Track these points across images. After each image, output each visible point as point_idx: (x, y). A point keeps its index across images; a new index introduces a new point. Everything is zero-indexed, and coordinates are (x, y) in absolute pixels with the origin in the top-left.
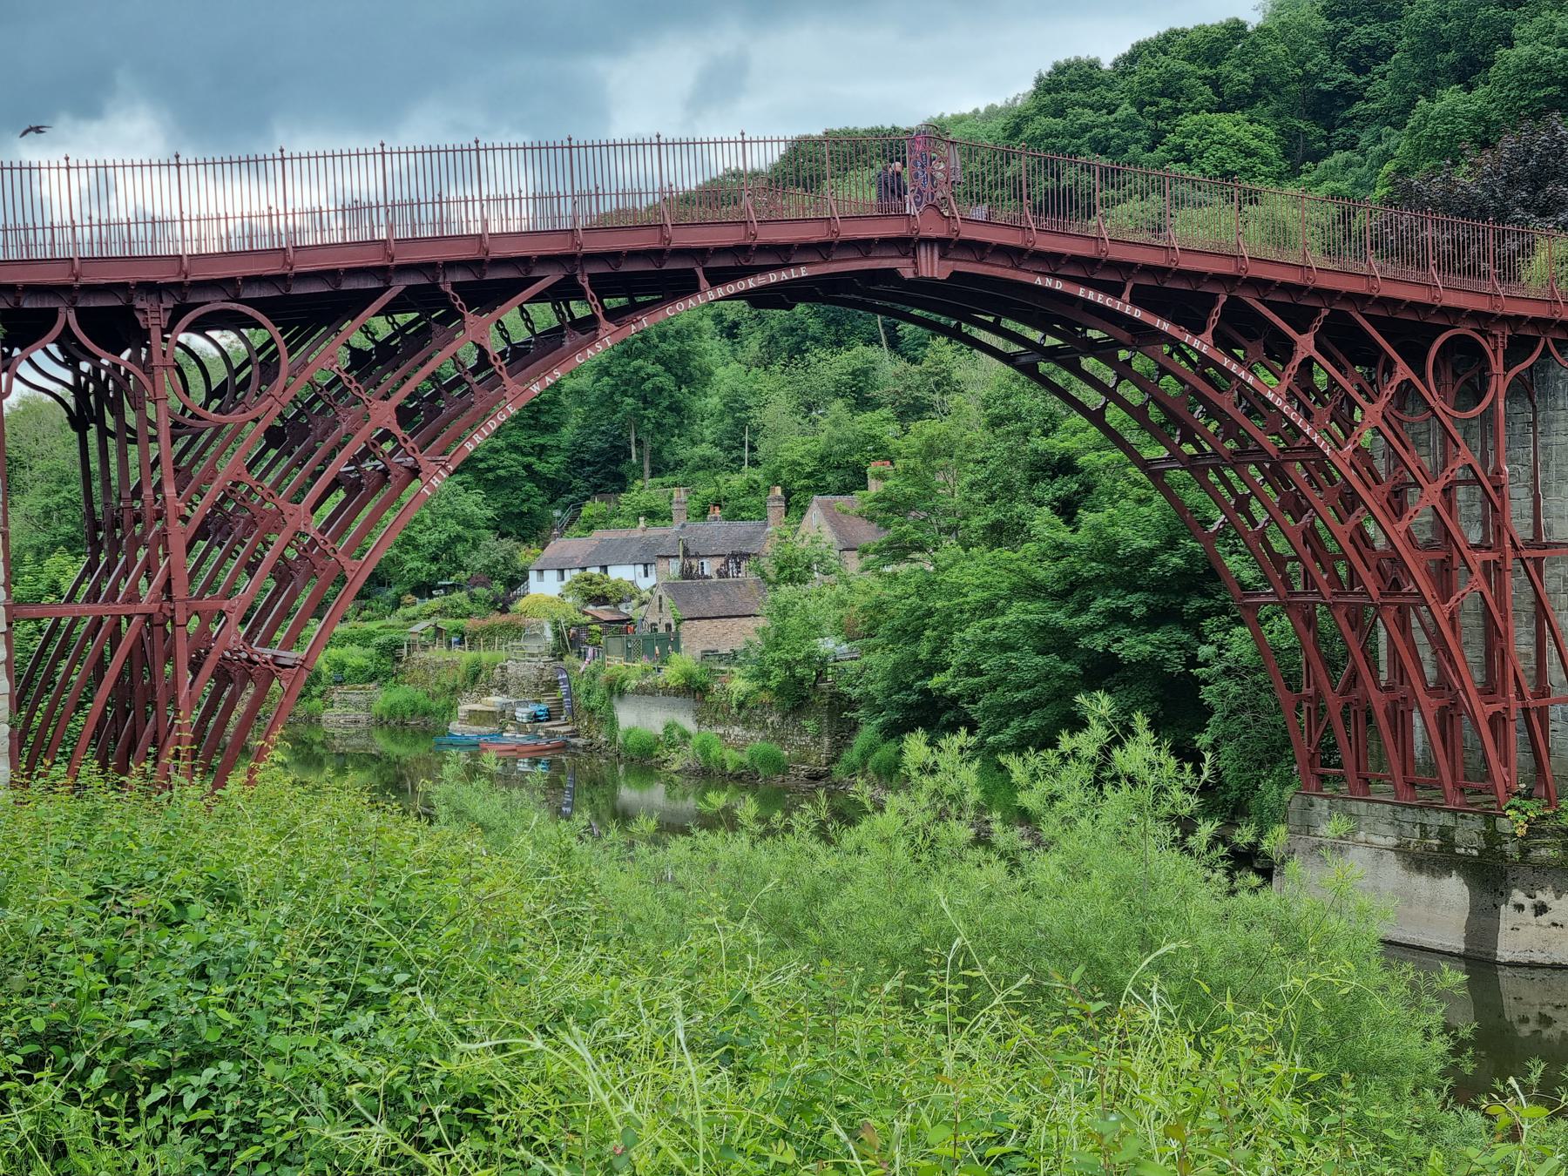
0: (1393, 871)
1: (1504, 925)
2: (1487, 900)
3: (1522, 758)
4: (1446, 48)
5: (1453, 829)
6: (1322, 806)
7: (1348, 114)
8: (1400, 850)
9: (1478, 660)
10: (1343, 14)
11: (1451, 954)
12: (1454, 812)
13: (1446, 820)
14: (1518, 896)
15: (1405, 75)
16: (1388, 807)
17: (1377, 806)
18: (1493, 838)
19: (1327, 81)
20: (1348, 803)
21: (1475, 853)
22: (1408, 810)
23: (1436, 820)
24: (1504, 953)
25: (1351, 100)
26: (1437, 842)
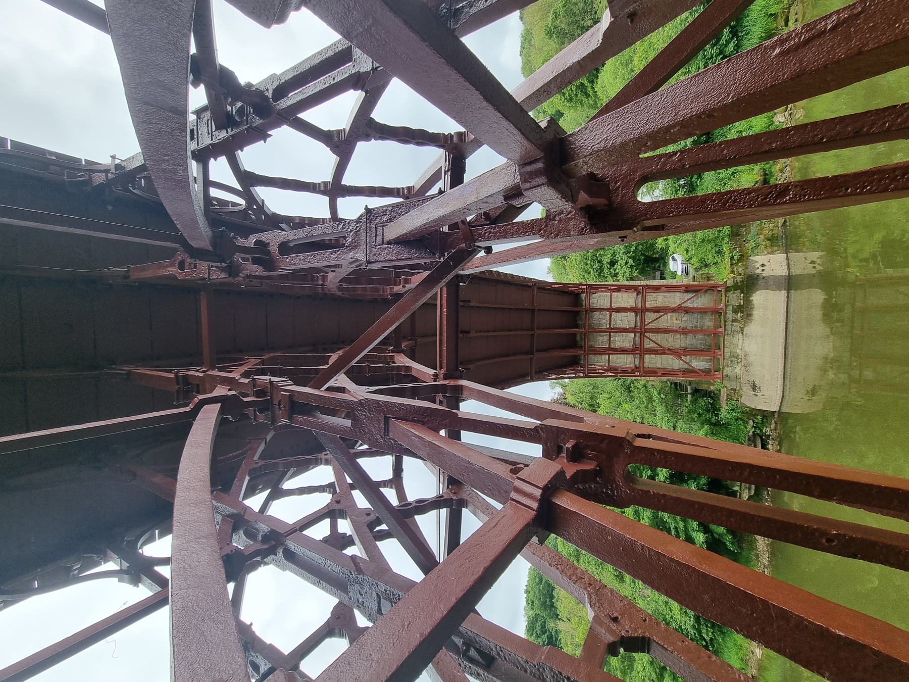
0: (752, 328)
1: (771, 274)
2: (761, 282)
3: (707, 320)
4: (546, 601)
5: (733, 306)
6: (727, 371)
7: (554, 639)
8: (742, 330)
9: (672, 336)
10: (533, 632)
11: (788, 297)
12: (726, 306)
13: (730, 309)
14: (759, 271)
15: (548, 615)
16: (726, 338)
17: (726, 343)
18: (736, 287)
19: (545, 641)
20: (725, 357)
21: (742, 295)
22: (727, 327)
23: (730, 315)
24: (784, 272)
25: (552, 636)
26: (739, 314)
